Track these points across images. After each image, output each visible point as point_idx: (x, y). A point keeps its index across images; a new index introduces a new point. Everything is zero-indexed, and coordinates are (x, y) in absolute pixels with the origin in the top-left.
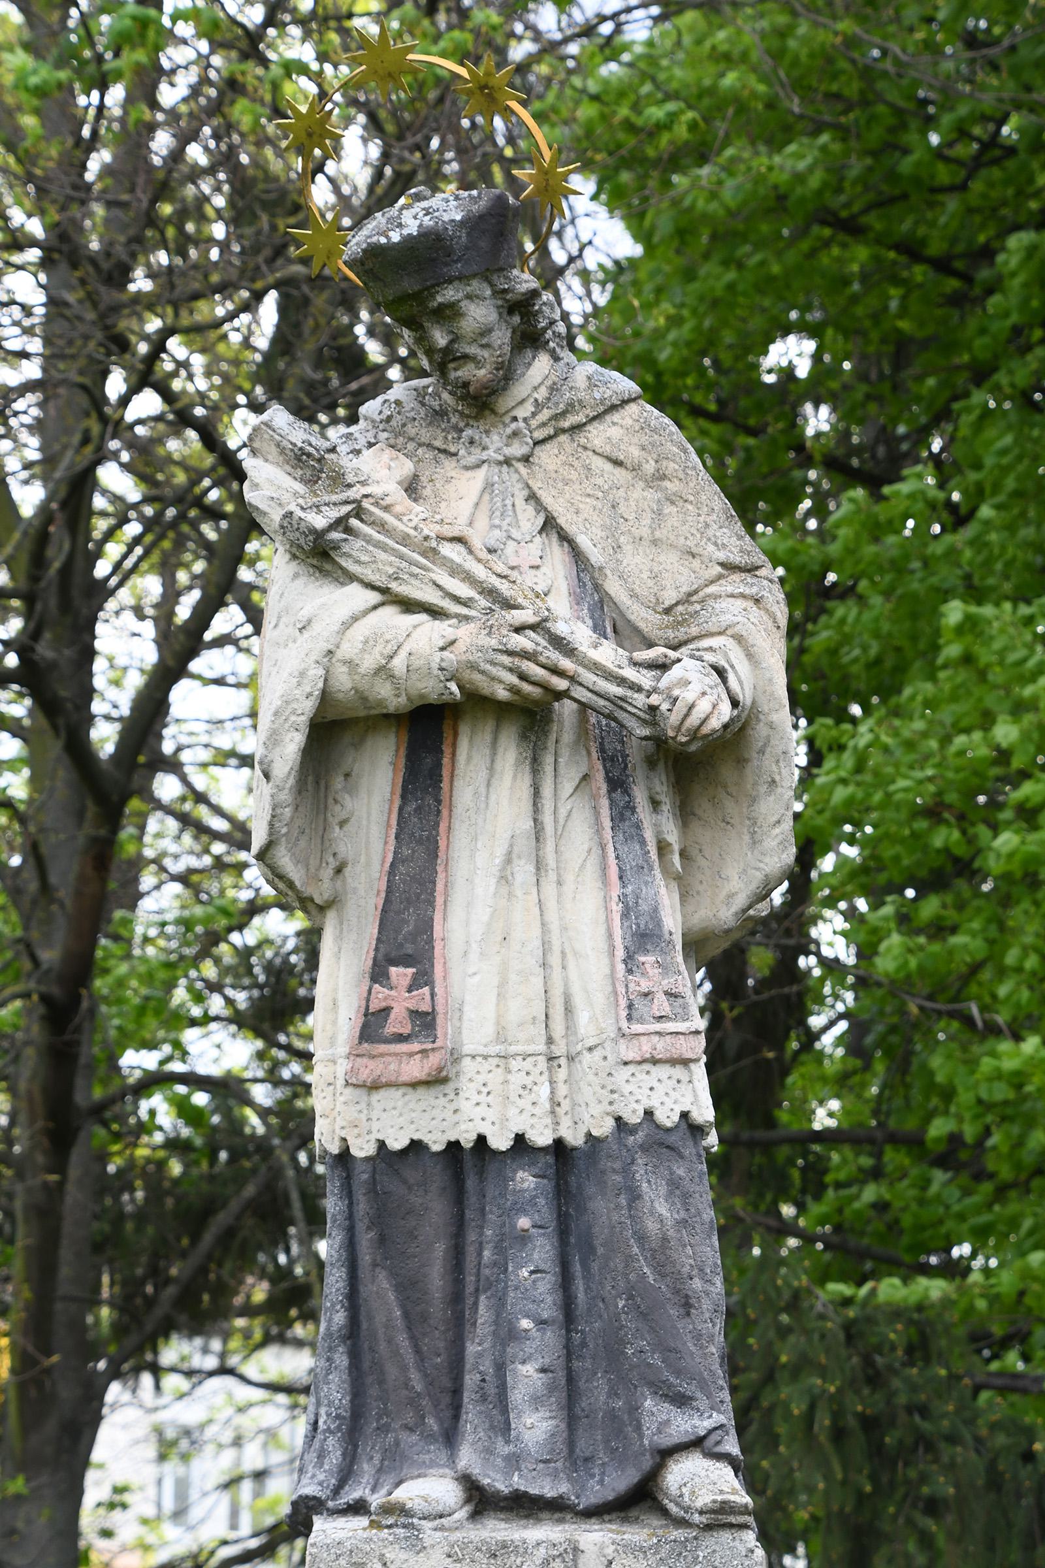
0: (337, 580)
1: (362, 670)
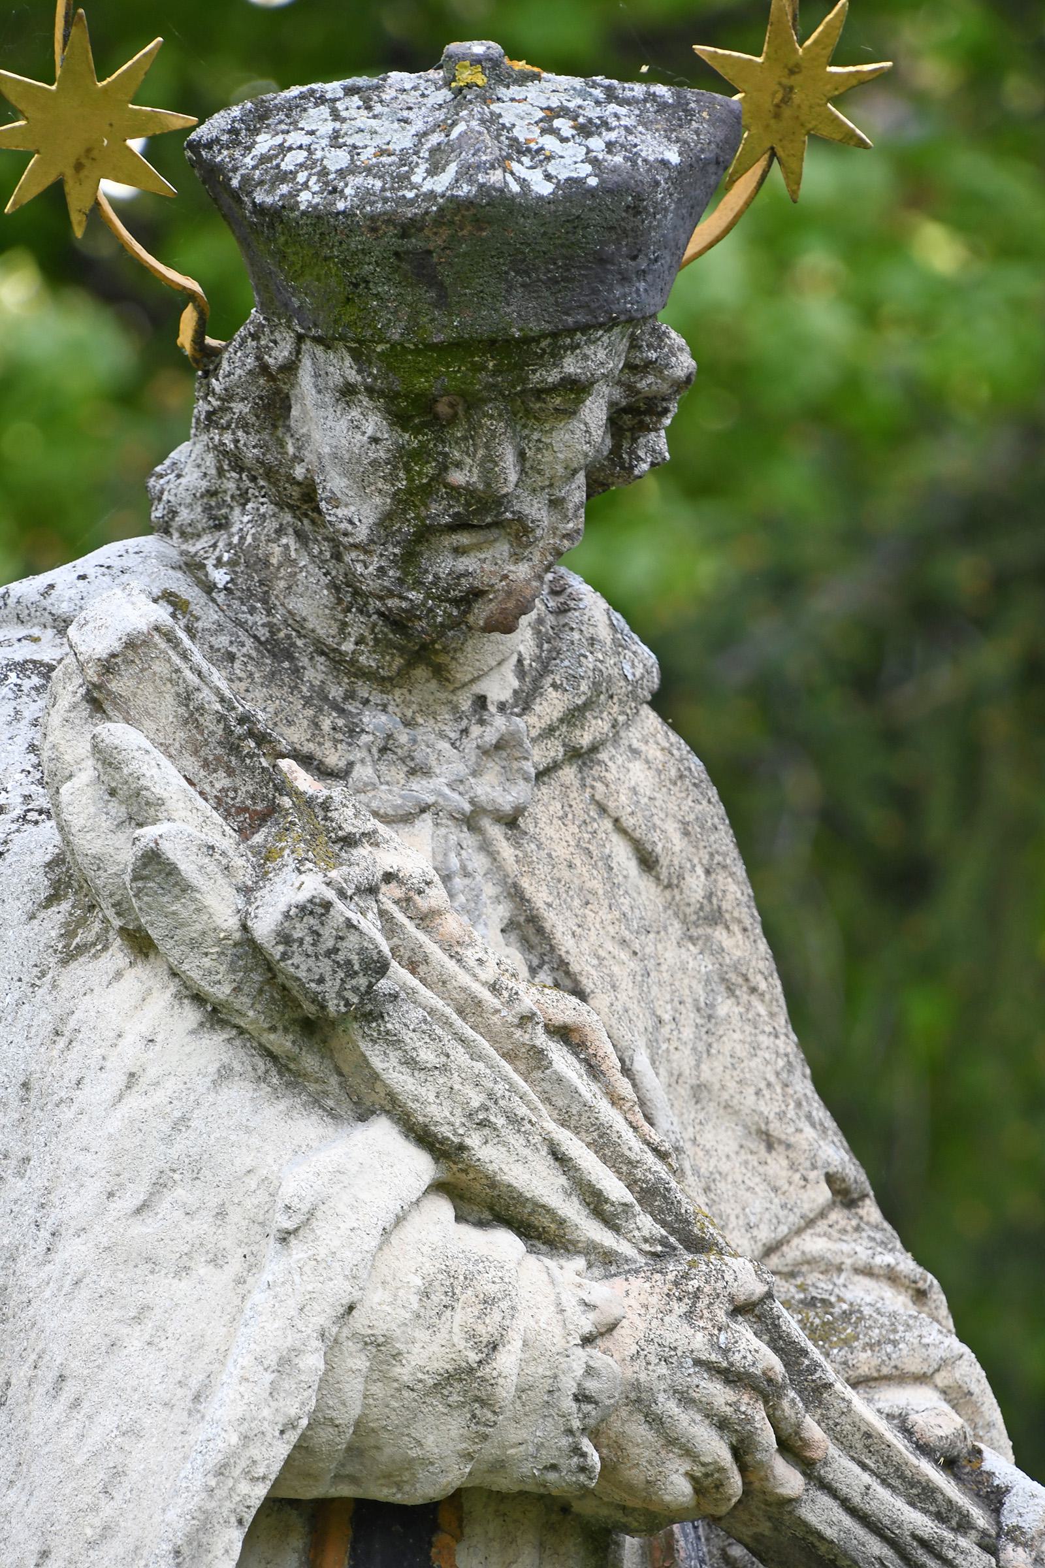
0: (316, 1102)
1: (404, 1373)
